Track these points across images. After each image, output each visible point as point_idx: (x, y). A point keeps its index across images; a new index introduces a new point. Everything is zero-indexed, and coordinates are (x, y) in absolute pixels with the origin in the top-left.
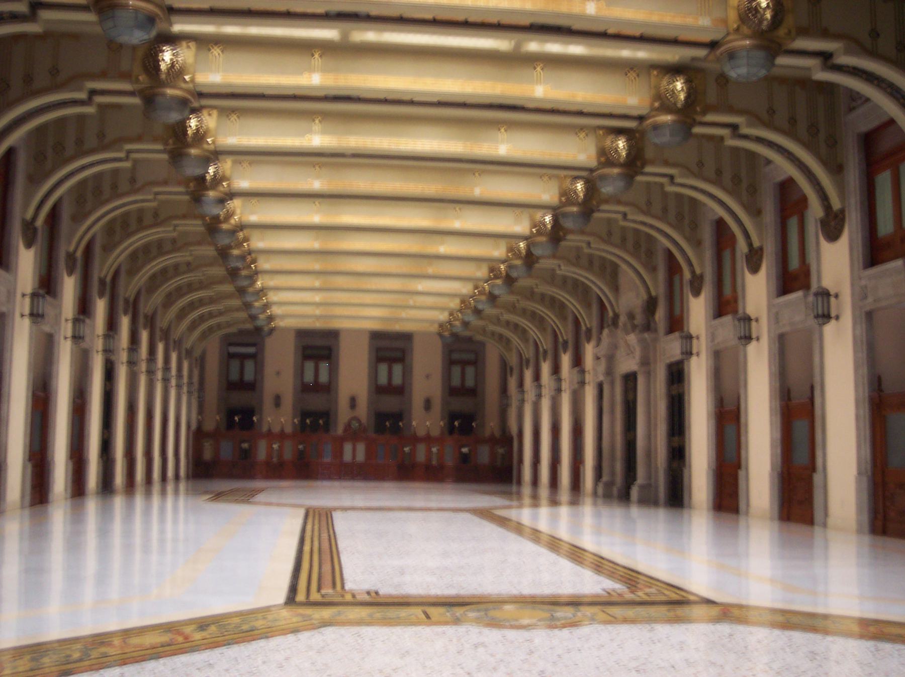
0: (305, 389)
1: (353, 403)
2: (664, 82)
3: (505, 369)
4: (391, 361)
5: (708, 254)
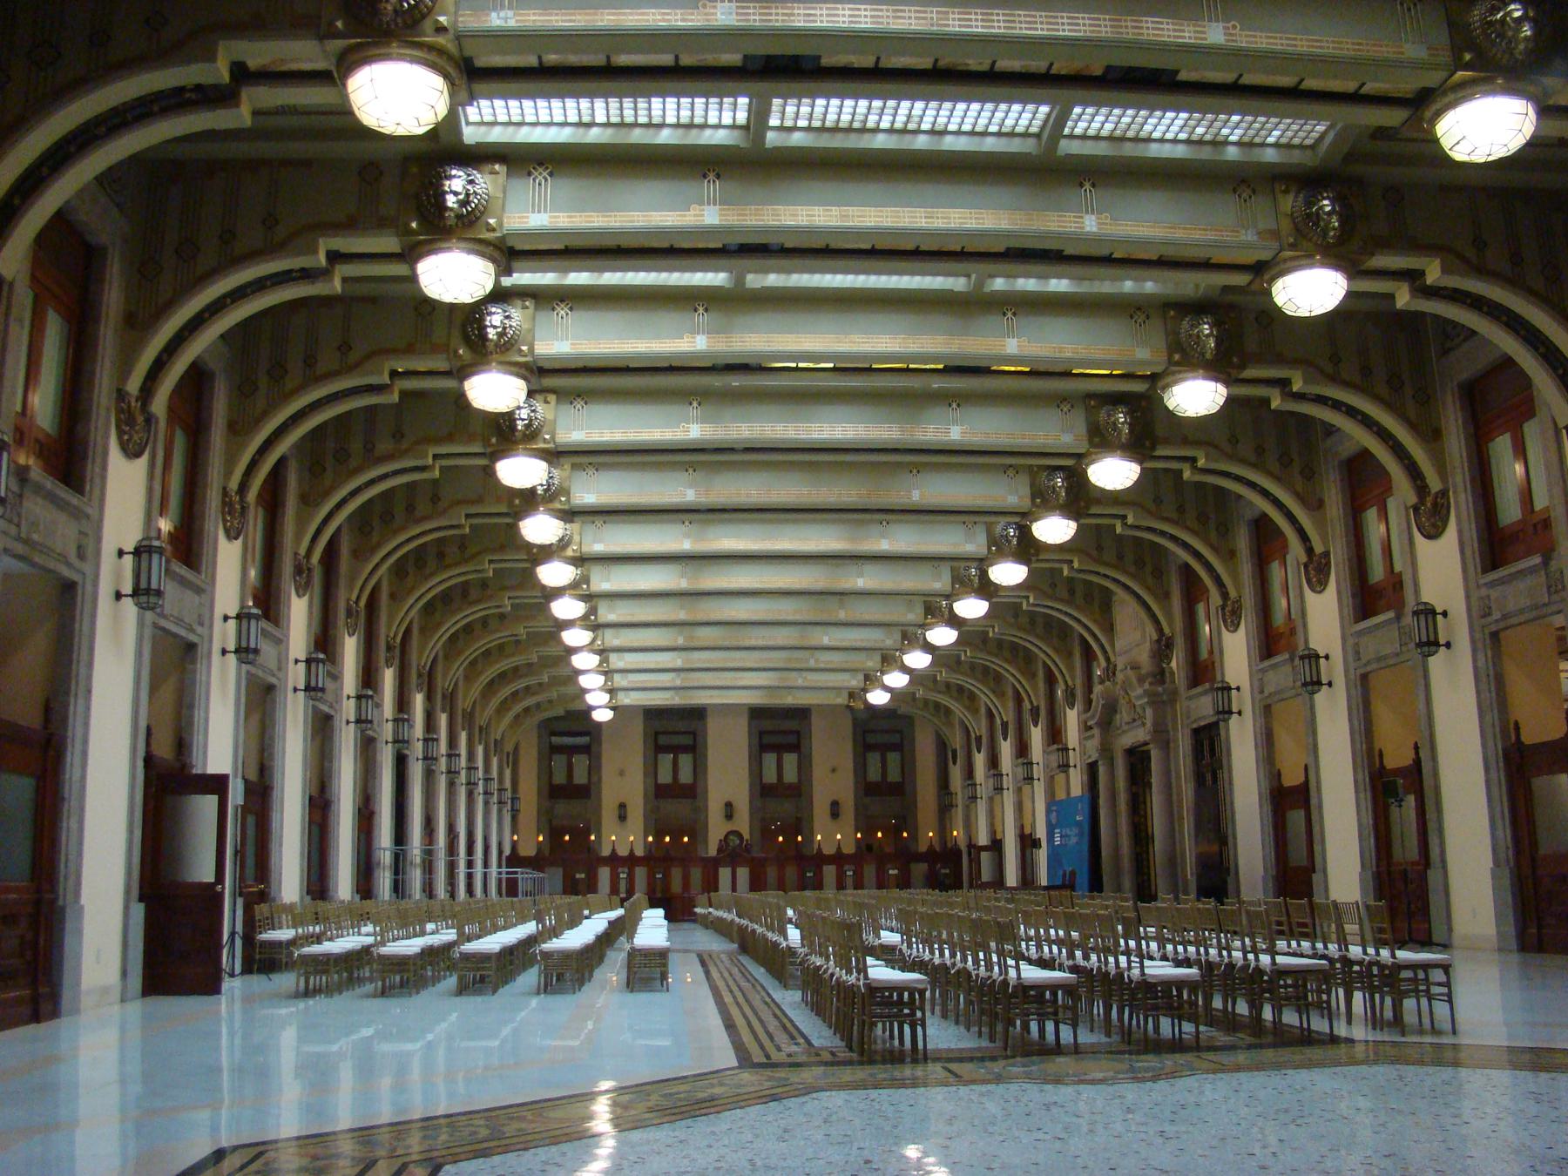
0: (660, 792)
2: (1185, 324)
3: (944, 753)
4: (779, 749)
5: (1246, 569)
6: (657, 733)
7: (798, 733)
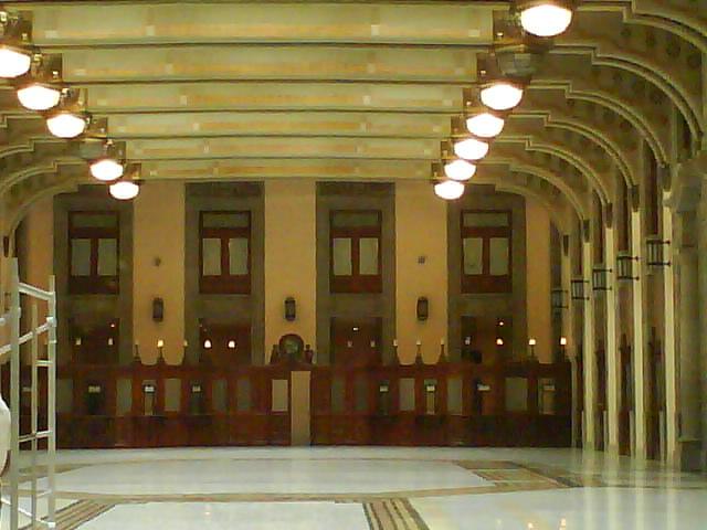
0: (206, 286)
1: (290, 309)
3: (558, 242)
4: (355, 235)
6: (201, 213)
7: (380, 213)
